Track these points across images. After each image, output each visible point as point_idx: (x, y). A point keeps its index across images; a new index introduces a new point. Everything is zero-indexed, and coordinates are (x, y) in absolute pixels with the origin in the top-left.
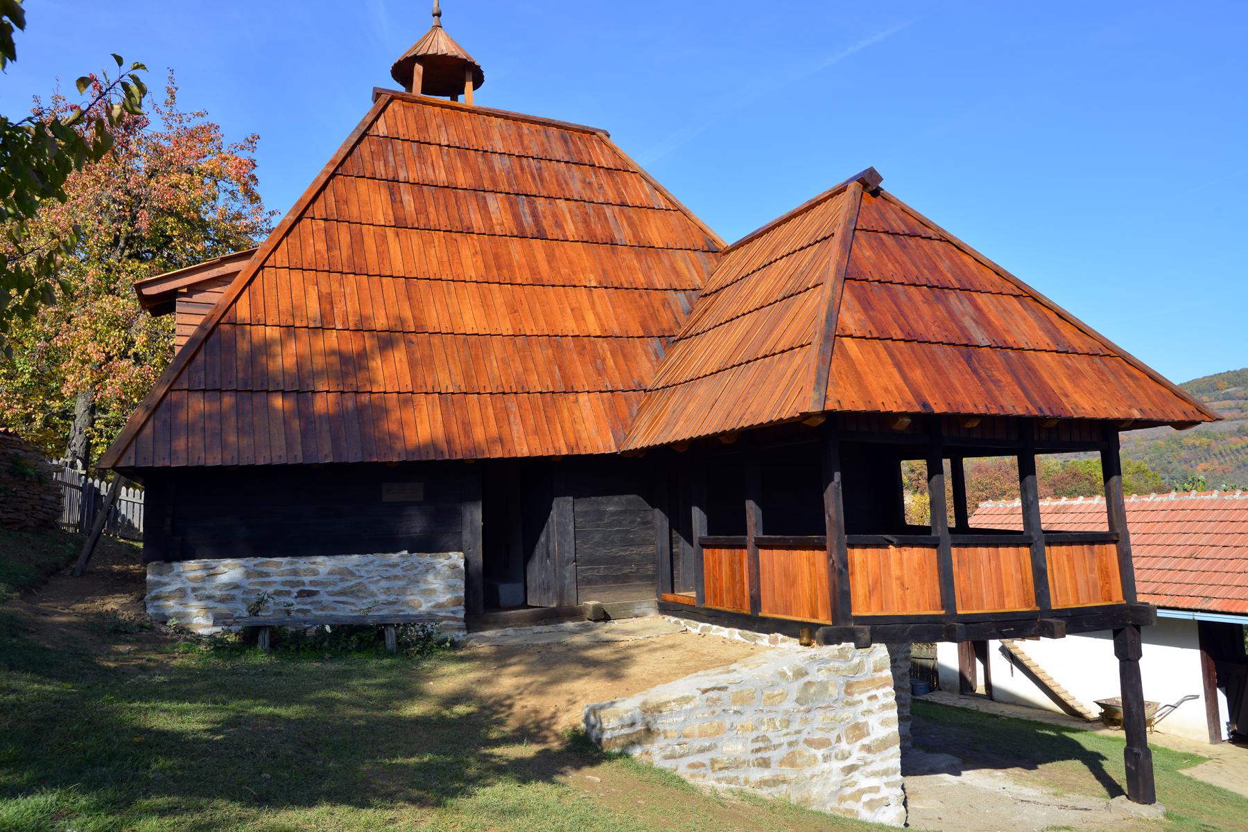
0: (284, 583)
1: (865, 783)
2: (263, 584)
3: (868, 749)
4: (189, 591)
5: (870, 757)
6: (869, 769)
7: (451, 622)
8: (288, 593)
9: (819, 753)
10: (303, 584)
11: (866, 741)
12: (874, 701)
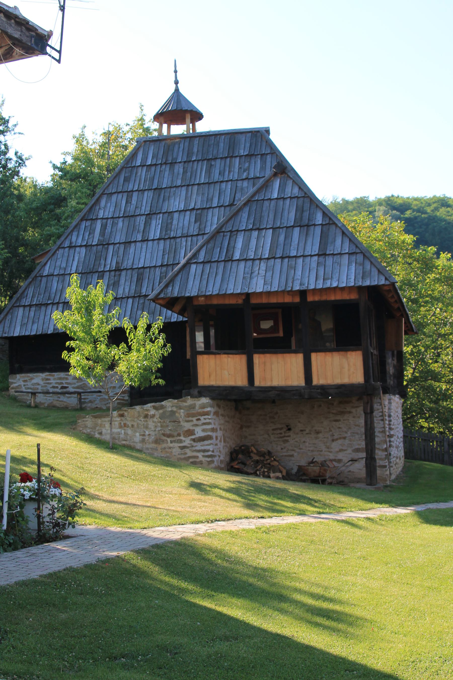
0: (56, 383)
1: (189, 453)
2: (48, 383)
3: (194, 440)
4: (23, 386)
5: (195, 444)
6: (194, 449)
7: (122, 401)
8: (57, 387)
9: (169, 440)
10: (63, 383)
11: (193, 437)
12: (199, 421)
